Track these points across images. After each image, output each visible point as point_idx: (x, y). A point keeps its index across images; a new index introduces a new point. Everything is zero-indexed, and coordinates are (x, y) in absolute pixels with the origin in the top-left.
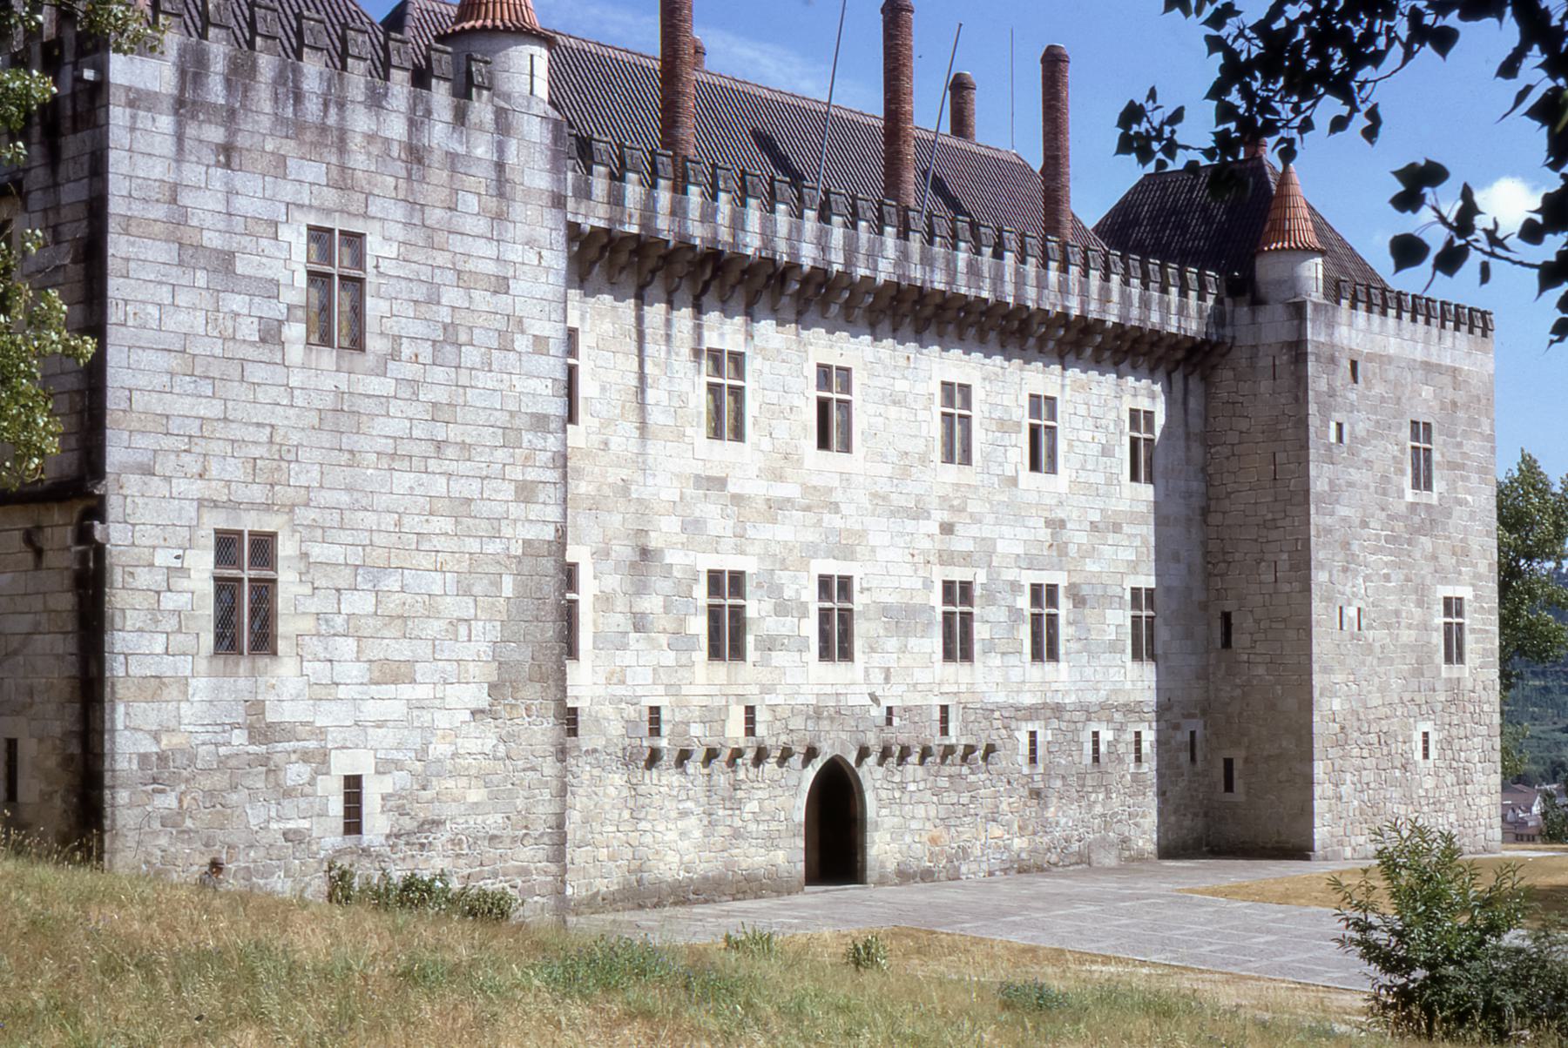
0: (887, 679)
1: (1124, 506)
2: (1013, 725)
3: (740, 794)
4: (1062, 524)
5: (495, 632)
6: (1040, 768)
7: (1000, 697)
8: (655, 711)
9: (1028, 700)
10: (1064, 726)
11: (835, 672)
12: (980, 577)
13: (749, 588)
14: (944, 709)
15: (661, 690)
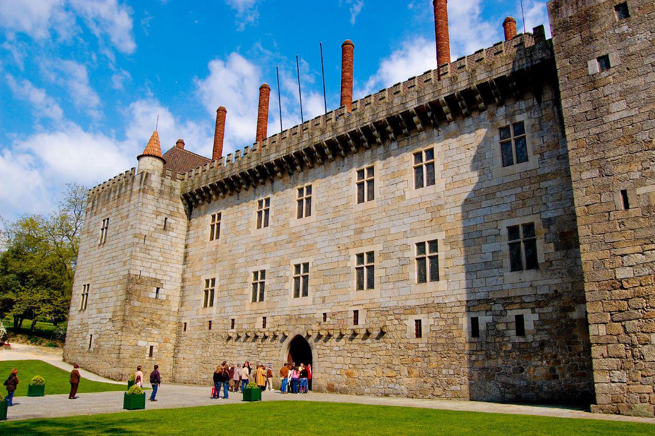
0: (324, 301)
1: (494, 183)
2: (403, 317)
3: (259, 349)
4: (440, 207)
5: (115, 299)
6: (424, 339)
7: (392, 304)
8: (233, 320)
9: (412, 303)
10: (445, 316)
11: (301, 300)
12: (377, 248)
13: (266, 275)
14: (356, 312)
15: (235, 314)
